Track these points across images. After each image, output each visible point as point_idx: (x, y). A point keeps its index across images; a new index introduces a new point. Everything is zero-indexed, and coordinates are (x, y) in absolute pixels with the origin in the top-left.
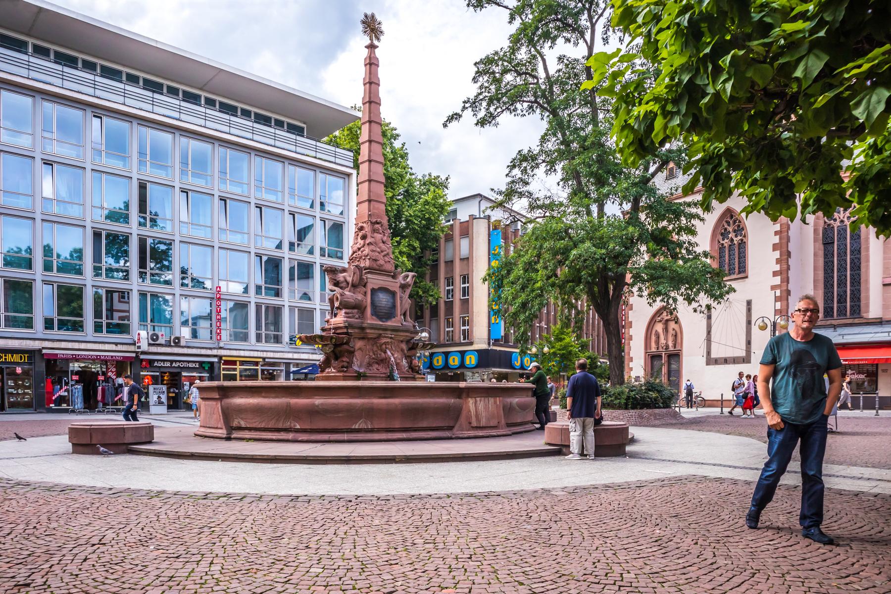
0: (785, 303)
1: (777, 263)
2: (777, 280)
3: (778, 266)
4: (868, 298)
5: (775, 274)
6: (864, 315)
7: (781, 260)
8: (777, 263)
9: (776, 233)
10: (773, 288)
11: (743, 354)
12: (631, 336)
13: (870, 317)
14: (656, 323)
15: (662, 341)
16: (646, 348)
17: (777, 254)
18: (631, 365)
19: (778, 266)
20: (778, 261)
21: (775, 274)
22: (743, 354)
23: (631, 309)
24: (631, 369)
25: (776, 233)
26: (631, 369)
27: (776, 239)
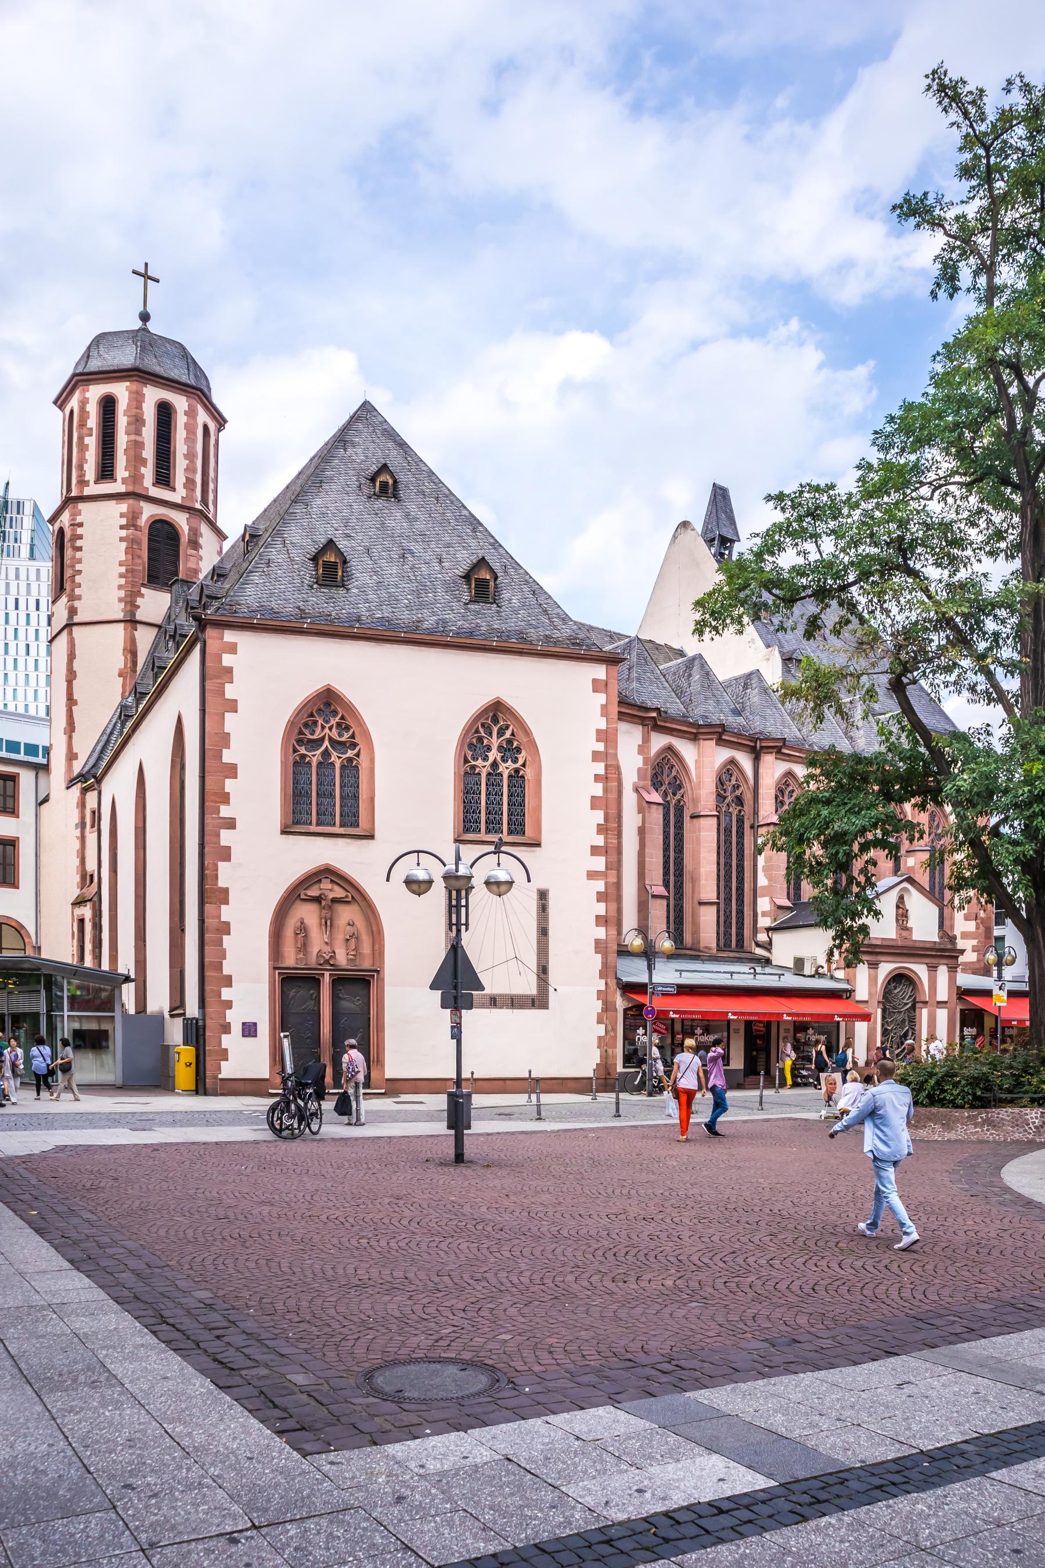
0: (613, 906)
1: (599, 832)
2: (599, 863)
3: (602, 837)
5: (595, 850)
7: (607, 830)
8: (599, 832)
9: (597, 778)
10: (592, 875)
11: (529, 987)
12: (228, 924)
14: (298, 902)
17: (599, 816)
18: (226, 994)
19: (602, 837)
20: (601, 829)
21: (595, 850)
22: (529, 987)
23: (227, 858)
24: (229, 1004)
25: (597, 778)
26: (229, 1004)
27: (598, 790)
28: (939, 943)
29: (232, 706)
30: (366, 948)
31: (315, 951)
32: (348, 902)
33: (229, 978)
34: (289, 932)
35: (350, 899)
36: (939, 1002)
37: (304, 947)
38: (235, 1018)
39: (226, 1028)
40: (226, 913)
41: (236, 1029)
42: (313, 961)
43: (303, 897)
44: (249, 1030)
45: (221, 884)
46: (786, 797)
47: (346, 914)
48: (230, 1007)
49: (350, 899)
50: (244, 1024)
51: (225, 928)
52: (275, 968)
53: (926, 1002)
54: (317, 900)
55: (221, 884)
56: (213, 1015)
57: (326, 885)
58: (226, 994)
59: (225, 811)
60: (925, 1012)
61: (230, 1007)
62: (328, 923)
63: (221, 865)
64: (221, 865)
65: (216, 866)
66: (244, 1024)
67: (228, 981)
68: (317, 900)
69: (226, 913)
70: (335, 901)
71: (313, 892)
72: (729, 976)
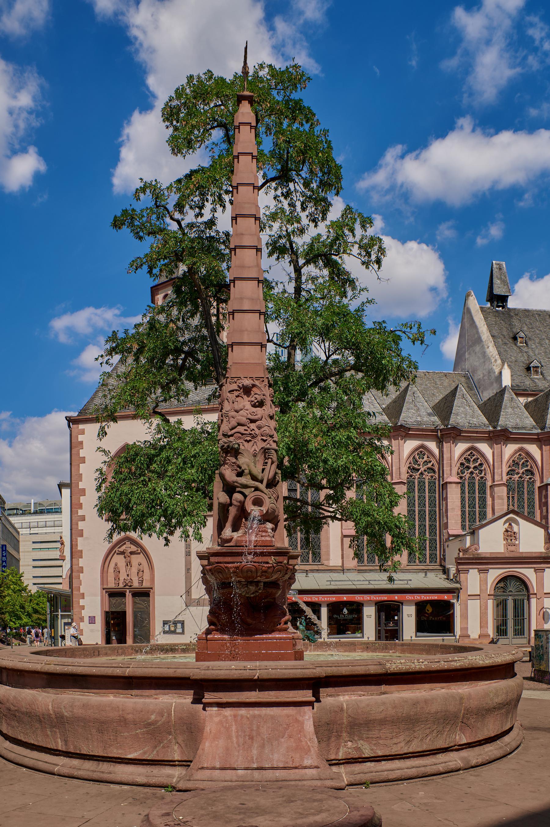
4: (328, 546)
6: (325, 562)
13: (331, 565)
15: (123, 576)
16: (102, 583)
18: (82, 602)
24: (83, 608)
26: (83, 608)
28: (546, 553)
29: (83, 460)
30: (147, 576)
31: (122, 579)
32: (139, 553)
33: (83, 594)
34: (111, 569)
35: (139, 551)
36: (545, 594)
37: (117, 578)
38: (85, 614)
39: (82, 619)
40: (82, 562)
41: (86, 619)
42: (121, 585)
43: (117, 552)
44: (92, 620)
45: (79, 548)
46: (471, 463)
47: (136, 559)
48: (84, 609)
49: (139, 551)
50: (89, 617)
51: (81, 570)
52: (104, 589)
53: (536, 594)
54: (123, 553)
55: (79, 548)
56: (76, 613)
57: (128, 544)
58: (82, 602)
59: (80, 513)
60: (533, 601)
61: (84, 609)
62: (129, 564)
63: (79, 539)
64: (79, 539)
65: (77, 539)
66: (89, 617)
67: (83, 596)
68: (123, 553)
69: (81, 562)
70: (132, 553)
71: (121, 549)
72: (367, 582)
